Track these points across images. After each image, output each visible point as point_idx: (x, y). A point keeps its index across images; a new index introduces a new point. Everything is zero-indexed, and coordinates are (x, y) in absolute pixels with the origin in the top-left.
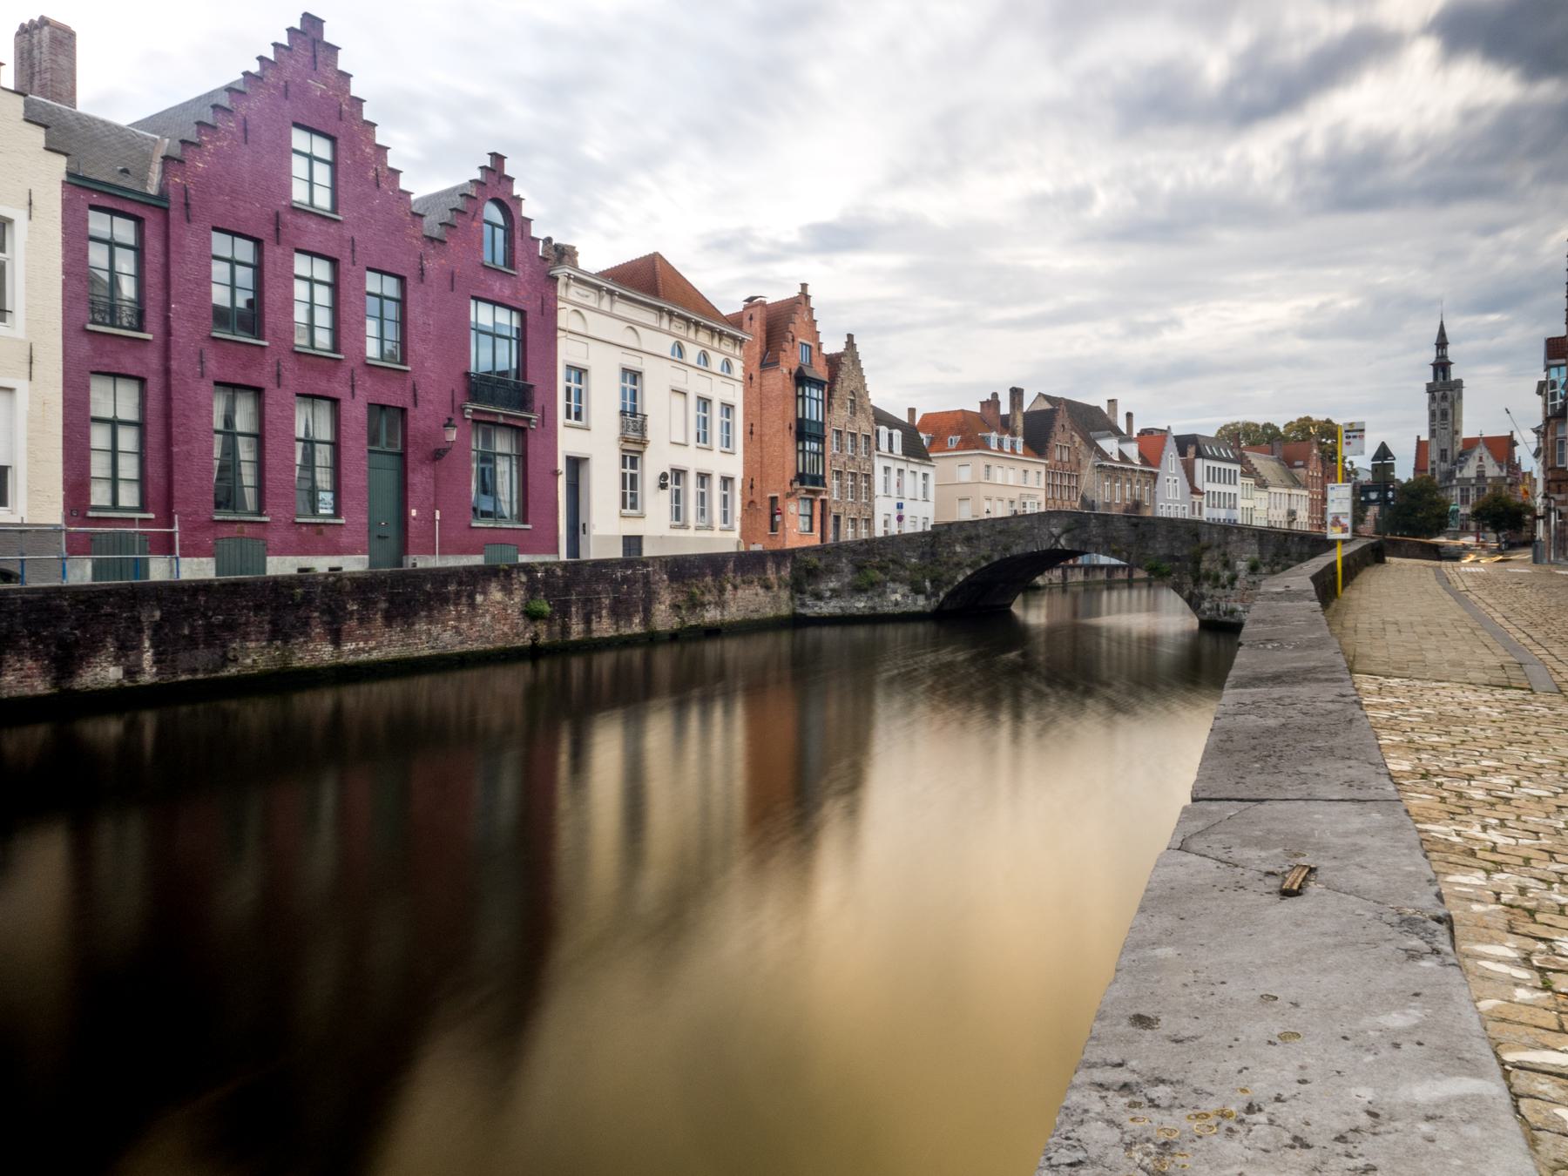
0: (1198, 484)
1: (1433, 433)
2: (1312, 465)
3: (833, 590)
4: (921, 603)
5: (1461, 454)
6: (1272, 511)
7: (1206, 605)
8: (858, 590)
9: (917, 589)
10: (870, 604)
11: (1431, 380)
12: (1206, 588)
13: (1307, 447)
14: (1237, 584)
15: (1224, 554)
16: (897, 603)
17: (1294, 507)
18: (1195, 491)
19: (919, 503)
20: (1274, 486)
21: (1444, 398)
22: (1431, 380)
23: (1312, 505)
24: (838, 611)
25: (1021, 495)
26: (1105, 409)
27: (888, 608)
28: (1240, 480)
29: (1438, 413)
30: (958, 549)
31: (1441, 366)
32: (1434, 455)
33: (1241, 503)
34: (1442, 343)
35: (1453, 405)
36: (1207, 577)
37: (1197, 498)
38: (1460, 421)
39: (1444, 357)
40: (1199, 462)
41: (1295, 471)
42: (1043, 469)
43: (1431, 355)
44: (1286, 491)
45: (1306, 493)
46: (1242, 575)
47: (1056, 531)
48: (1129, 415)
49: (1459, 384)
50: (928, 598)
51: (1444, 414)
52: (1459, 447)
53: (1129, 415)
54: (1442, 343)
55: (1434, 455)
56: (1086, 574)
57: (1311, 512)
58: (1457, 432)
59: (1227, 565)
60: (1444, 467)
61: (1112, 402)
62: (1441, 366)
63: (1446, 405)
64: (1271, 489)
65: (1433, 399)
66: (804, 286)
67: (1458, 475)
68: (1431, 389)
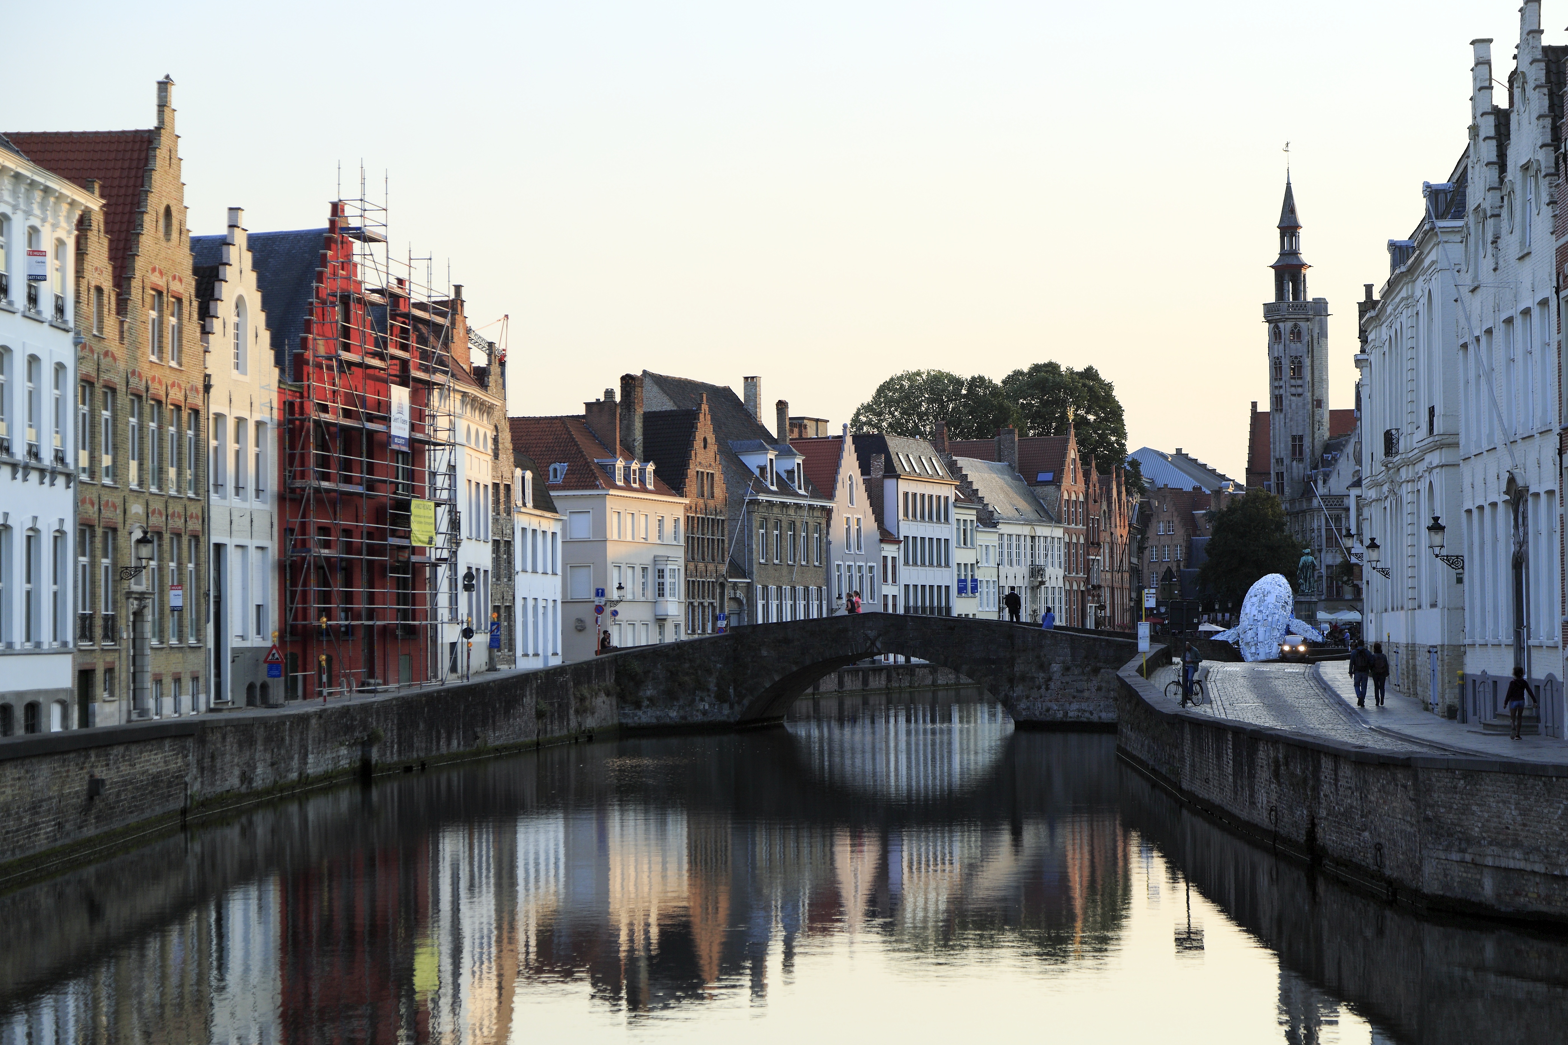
0: (889, 524)
1: (1277, 400)
2: (1067, 481)
3: (650, 699)
4: (725, 713)
5: (1328, 447)
6: (1005, 569)
7: (1022, 705)
8: (670, 696)
9: (722, 697)
10: (682, 713)
11: (1272, 299)
12: (1019, 690)
13: (1047, 421)
14: (1052, 685)
15: (1038, 657)
16: (705, 713)
17: (1040, 561)
18: (887, 537)
19: (549, 577)
20: (1009, 521)
21: (1297, 334)
22: (1272, 299)
23: (1068, 554)
24: (654, 721)
25: (655, 560)
26: (740, 392)
27: (699, 718)
28: (955, 514)
29: (1286, 364)
30: (764, 653)
31: (1289, 271)
32: (1281, 447)
33: (961, 556)
34: (1289, 227)
35: (1311, 351)
36: (1023, 678)
37: (890, 550)
38: (1324, 381)
39: (1295, 253)
40: (889, 483)
41: (1039, 490)
42: (681, 514)
43: (1271, 250)
44: (1026, 530)
45: (1058, 532)
46: (1056, 676)
47: (872, 634)
48: (782, 406)
49: (1320, 307)
50: (731, 707)
51: (1297, 369)
52: (1324, 432)
53: (782, 406)
54: (1289, 227)
55: (1281, 447)
56: (889, 679)
57: (1068, 569)
58: (1319, 403)
59: (1043, 667)
60: (1298, 469)
61: (751, 382)
62: (1289, 271)
63: (1297, 348)
64: (1003, 529)
65: (1276, 335)
66: (458, 288)
67: (1321, 490)
68: (1271, 313)
